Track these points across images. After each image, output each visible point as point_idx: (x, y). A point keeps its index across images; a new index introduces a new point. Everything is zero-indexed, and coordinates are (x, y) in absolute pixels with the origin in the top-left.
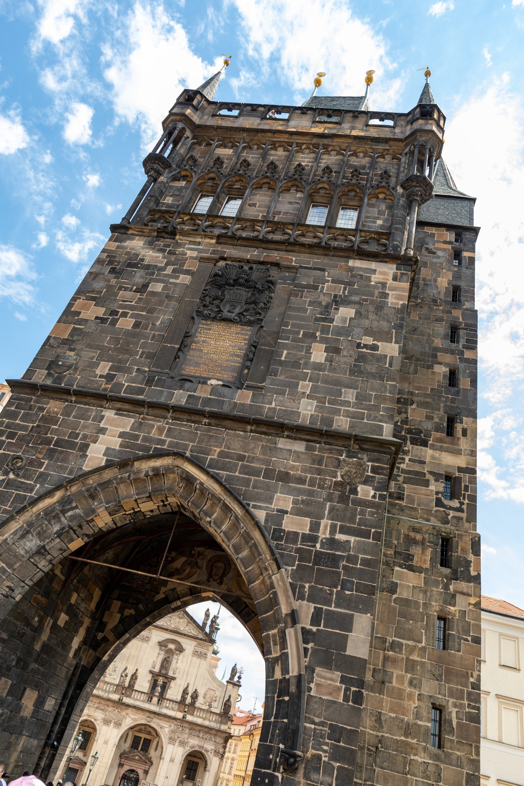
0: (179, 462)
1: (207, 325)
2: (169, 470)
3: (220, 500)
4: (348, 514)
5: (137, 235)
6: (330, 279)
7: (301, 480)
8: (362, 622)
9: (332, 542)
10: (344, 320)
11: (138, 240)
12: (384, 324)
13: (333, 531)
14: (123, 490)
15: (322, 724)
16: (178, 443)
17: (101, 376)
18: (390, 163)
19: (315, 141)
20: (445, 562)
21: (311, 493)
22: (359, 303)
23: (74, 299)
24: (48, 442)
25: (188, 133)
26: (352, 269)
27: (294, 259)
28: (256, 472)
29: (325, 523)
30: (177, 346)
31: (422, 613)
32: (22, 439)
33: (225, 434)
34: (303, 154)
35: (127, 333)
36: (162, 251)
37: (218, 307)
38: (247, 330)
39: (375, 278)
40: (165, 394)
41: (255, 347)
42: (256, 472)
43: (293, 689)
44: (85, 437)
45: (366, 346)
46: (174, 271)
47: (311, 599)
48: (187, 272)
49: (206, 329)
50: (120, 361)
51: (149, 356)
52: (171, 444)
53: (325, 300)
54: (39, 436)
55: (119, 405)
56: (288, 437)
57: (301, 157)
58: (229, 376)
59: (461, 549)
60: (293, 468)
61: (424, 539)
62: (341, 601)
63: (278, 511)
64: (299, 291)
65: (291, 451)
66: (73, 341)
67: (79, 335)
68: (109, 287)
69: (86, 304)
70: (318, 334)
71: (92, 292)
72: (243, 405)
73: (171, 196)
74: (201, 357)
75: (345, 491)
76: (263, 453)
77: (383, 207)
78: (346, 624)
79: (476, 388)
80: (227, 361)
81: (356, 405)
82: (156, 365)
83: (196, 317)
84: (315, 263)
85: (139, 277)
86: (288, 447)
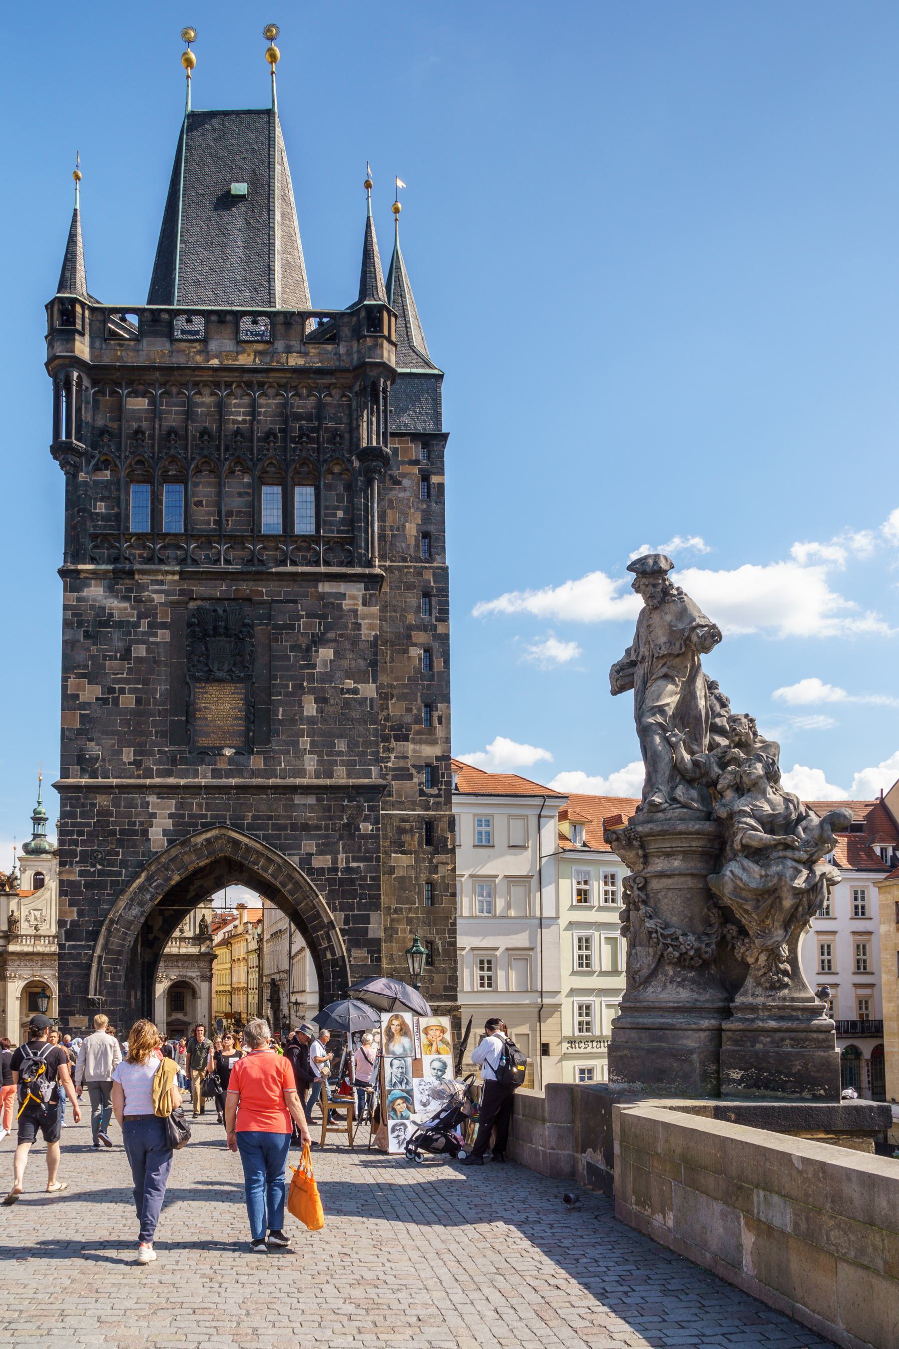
0: (224, 831)
1: (203, 688)
2: (217, 838)
3: (263, 855)
4: (356, 846)
5: (91, 579)
6: (304, 613)
7: (318, 828)
8: (374, 917)
9: (348, 869)
10: (325, 663)
11: (96, 586)
12: (361, 663)
13: (348, 862)
14: (186, 859)
15: (361, 977)
16: (217, 815)
17: (130, 764)
18: (340, 405)
19: (246, 377)
20: (429, 842)
21: (327, 836)
22: (336, 641)
23: (65, 679)
24: (114, 833)
25: (86, 383)
26: (322, 596)
27: (264, 590)
28: (284, 828)
29: (341, 856)
30: (184, 719)
31: (414, 885)
32: (90, 834)
33: (252, 799)
34: (236, 398)
35: (133, 712)
36: (126, 598)
37: (207, 665)
38: (241, 688)
39: (346, 604)
40: (191, 772)
41: (253, 707)
42: (284, 828)
43: (340, 963)
44: (141, 824)
45: (349, 691)
46: (150, 625)
47: (341, 910)
48: (164, 626)
49: (203, 693)
50: (140, 745)
51: (163, 734)
52: (212, 817)
53: (304, 642)
54: (102, 827)
55: (157, 790)
56: (301, 794)
57: (236, 406)
58: (238, 741)
59: (443, 825)
60: (310, 818)
61: (412, 827)
62: (361, 906)
63: (307, 854)
64: (278, 634)
65: (305, 805)
66: (87, 730)
67: (89, 722)
68: (93, 658)
69: (79, 684)
70: (305, 684)
71: (78, 667)
72: (258, 770)
73: (102, 500)
74: (208, 726)
75: (351, 828)
76: (285, 810)
77: (341, 489)
78: (366, 920)
79: (449, 669)
80: (232, 726)
81: (348, 754)
82: (173, 743)
83: (188, 680)
84: (286, 593)
85: (117, 640)
86: (303, 802)
